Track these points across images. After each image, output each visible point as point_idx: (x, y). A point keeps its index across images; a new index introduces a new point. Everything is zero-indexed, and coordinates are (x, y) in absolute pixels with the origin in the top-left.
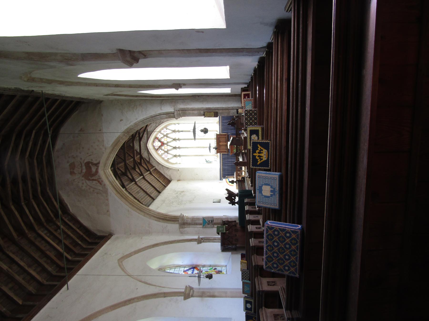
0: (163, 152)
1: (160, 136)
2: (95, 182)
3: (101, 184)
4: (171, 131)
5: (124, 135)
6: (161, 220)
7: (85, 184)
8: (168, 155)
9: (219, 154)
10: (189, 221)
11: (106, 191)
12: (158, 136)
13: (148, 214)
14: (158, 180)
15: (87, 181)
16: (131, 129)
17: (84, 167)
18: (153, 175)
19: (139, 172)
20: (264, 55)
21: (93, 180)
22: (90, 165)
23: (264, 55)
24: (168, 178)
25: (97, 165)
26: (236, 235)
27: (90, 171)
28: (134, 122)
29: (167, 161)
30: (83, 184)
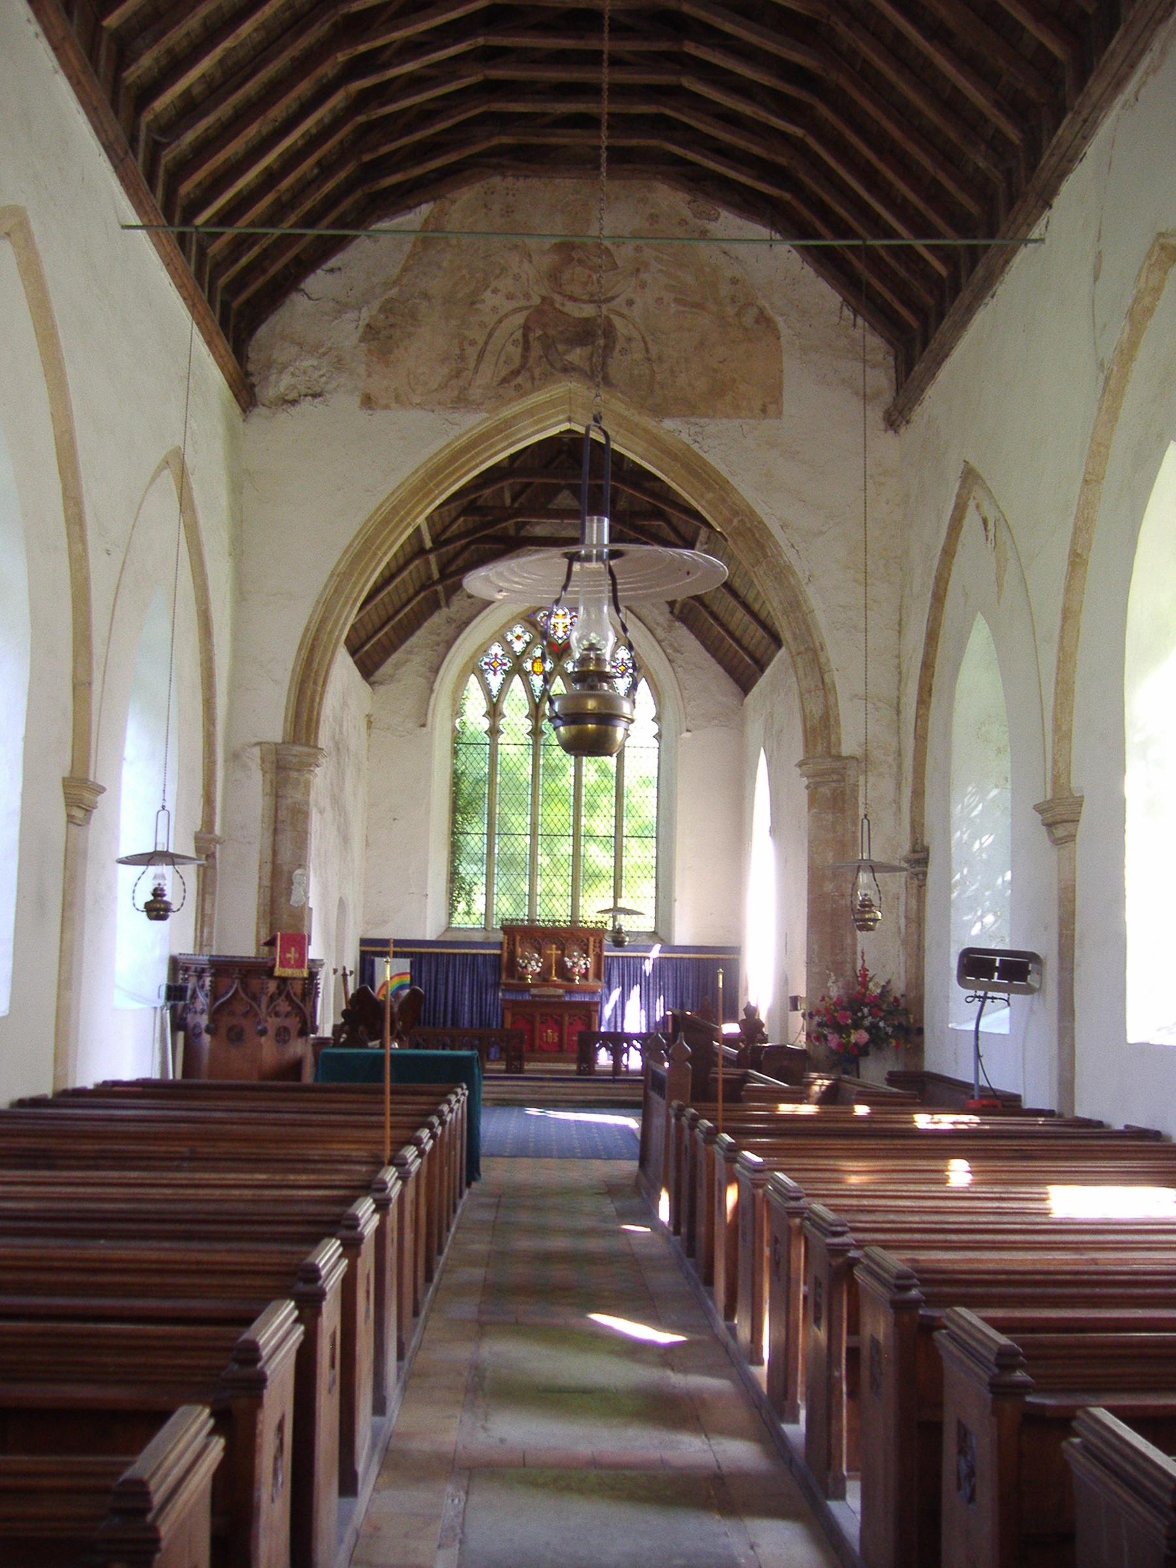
0: (518, 646)
2: (516, 352)
3: (505, 380)
5: (736, 513)
6: (304, 653)
7: (509, 306)
8: (500, 677)
9: (500, 937)
10: (293, 795)
11: (462, 402)
13: (337, 591)
14: (390, 619)
15: (519, 319)
16: (762, 547)
17: (588, 311)
18: (417, 593)
19: (448, 534)
22: (601, 342)
24: (386, 669)
26: (263, 1032)
27: (568, 339)
28: (797, 566)
30: (510, 297)
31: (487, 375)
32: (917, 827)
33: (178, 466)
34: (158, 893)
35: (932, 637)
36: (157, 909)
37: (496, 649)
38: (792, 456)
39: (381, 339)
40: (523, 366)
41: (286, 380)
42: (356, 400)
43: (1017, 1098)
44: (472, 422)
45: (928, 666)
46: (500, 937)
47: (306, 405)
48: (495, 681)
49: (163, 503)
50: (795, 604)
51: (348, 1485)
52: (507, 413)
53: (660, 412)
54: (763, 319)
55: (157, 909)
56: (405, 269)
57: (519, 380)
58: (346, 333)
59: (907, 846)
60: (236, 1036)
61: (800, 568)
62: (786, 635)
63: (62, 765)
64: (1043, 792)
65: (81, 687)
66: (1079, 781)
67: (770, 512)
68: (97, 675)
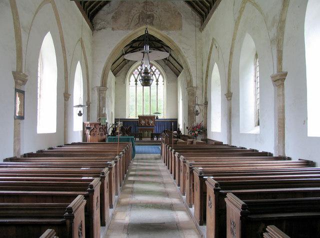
1: (154, 68)
4: (157, 78)
9: (138, 118)
11: (129, 29)
12: (154, 67)
17: (150, 13)
20: (274, 156)
21: (139, 20)
23: (274, 156)
25: (152, 24)
27: (147, 18)
29: (132, 73)
30: (136, 11)
31: (133, 24)
32: (206, 98)
33: (81, 41)
34: (80, 112)
35: (208, 67)
36: (80, 114)
37: (136, 70)
38: (183, 38)
39: (115, 18)
40: (139, 23)
41: (99, 26)
42: (111, 29)
43: (222, 143)
44: (130, 32)
45: (207, 72)
46: (138, 118)
47: (103, 30)
48: (136, 76)
49: (79, 47)
50: (185, 62)
51: (111, 207)
52: (136, 31)
53: (162, 30)
54: (179, 13)
55: (80, 114)
56: (119, 7)
57: (138, 25)
58: (110, 16)
59: (204, 102)
60: (94, 135)
61: (186, 55)
62: (184, 67)
63: (63, 91)
64: (226, 92)
65: (66, 78)
66: (232, 91)
67: (181, 46)
68: (69, 76)
